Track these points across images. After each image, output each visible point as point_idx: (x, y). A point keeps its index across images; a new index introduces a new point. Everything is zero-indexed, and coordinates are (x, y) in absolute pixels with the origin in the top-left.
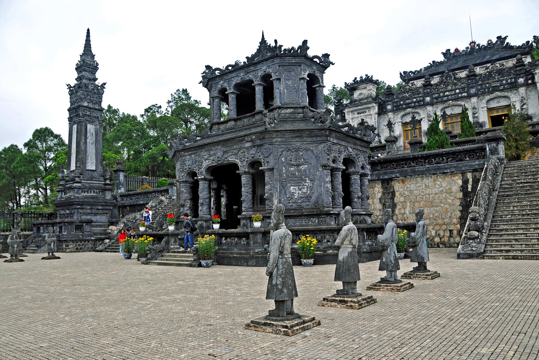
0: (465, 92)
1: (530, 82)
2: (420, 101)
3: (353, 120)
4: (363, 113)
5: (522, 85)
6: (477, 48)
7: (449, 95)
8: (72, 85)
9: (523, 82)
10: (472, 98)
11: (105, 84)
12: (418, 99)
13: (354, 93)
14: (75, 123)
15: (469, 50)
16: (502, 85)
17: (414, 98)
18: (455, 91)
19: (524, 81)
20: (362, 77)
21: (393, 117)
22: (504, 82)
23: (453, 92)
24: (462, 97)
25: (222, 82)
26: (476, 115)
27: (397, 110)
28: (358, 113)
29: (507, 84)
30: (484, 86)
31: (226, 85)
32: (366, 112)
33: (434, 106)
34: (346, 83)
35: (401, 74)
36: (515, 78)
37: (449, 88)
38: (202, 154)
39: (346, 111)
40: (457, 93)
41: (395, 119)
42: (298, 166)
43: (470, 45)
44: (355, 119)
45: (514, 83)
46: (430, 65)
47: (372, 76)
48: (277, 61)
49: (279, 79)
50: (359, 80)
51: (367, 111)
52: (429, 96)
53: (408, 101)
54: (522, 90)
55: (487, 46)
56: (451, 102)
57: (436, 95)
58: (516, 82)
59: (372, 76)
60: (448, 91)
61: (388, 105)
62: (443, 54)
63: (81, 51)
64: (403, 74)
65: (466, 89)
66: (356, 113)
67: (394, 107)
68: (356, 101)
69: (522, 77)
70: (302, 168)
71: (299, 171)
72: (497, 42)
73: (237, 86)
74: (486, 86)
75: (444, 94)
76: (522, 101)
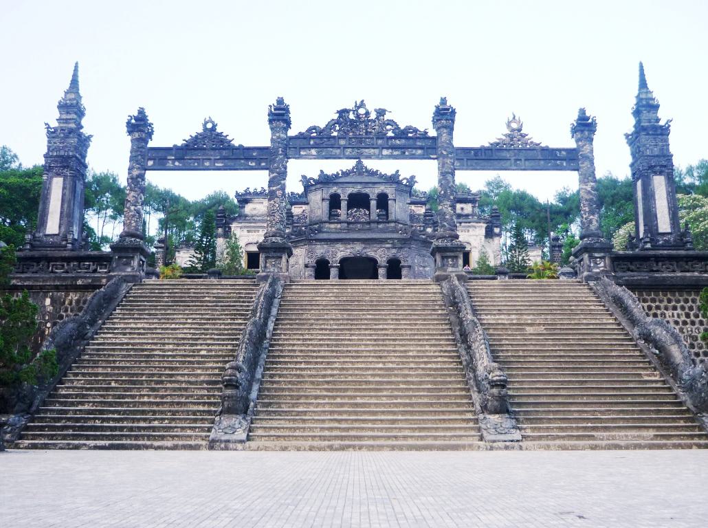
4: (255, 231)
8: (52, 126)
11: (92, 136)
14: (58, 175)
25: (335, 188)
28: (248, 231)
31: (339, 191)
36: (423, 226)
38: (337, 246)
42: (424, 267)
48: (394, 186)
49: (395, 200)
58: (424, 230)
63: (67, 86)
66: (245, 230)
68: (246, 216)
70: (427, 269)
71: (425, 271)
73: (351, 196)
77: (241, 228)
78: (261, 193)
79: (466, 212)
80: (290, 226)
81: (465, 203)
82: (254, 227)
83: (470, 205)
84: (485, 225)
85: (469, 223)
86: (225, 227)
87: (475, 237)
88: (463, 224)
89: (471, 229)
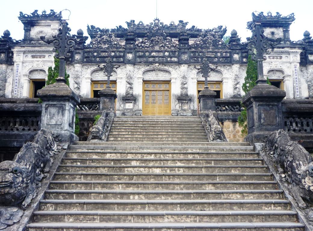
0: (175, 57)
1: (245, 60)
2: (120, 57)
3: (24, 64)
4: (40, 57)
5: (237, 62)
6: (161, 26)
7: (157, 57)
9: (238, 59)
10: (182, 65)
12: (118, 54)
13: (32, 29)
15: (153, 26)
16: (216, 58)
17: (113, 52)
18: (164, 53)
19: (239, 58)
20: (45, 12)
21: (80, 70)
22: (219, 54)
23: (161, 54)
24: (172, 62)
26: (185, 86)
27: (87, 62)
28: (33, 57)
29: (222, 57)
30: (197, 54)
32: (44, 57)
33: (136, 66)
34: (21, 13)
35: (88, 27)
36: (230, 53)
37: (157, 48)
39: (15, 50)
40: (166, 56)
41: (83, 73)
43: (154, 21)
44: (27, 64)
45: (228, 57)
46: (116, 28)
47: (61, 12)
50: (41, 14)
51: (47, 55)
52: (131, 53)
53: (103, 54)
54: (236, 67)
55: (170, 27)
56: (157, 64)
57: (141, 54)
58: (231, 57)
59: (61, 12)
60: (156, 51)
61: (76, 53)
62: (127, 23)
64: (90, 28)
65: (177, 53)
66: (30, 55)
67: (84, 57)
68: (32, 39)
69: (238, 54)
72: (179, 25)
74: (199, 55)
75: (150, 54)
76: (235, 79)
77: (24, 52)
78: (50, 16)
79: (277, 37)
80: (80, 51)
81: (276, 27)
82: (39, 52)
83: (281, 29)
84: (300, 51)
85: (283, 48)
86: (9, 53)
87: (289, 65)
88: (275, 50)
89: (284, 56)
